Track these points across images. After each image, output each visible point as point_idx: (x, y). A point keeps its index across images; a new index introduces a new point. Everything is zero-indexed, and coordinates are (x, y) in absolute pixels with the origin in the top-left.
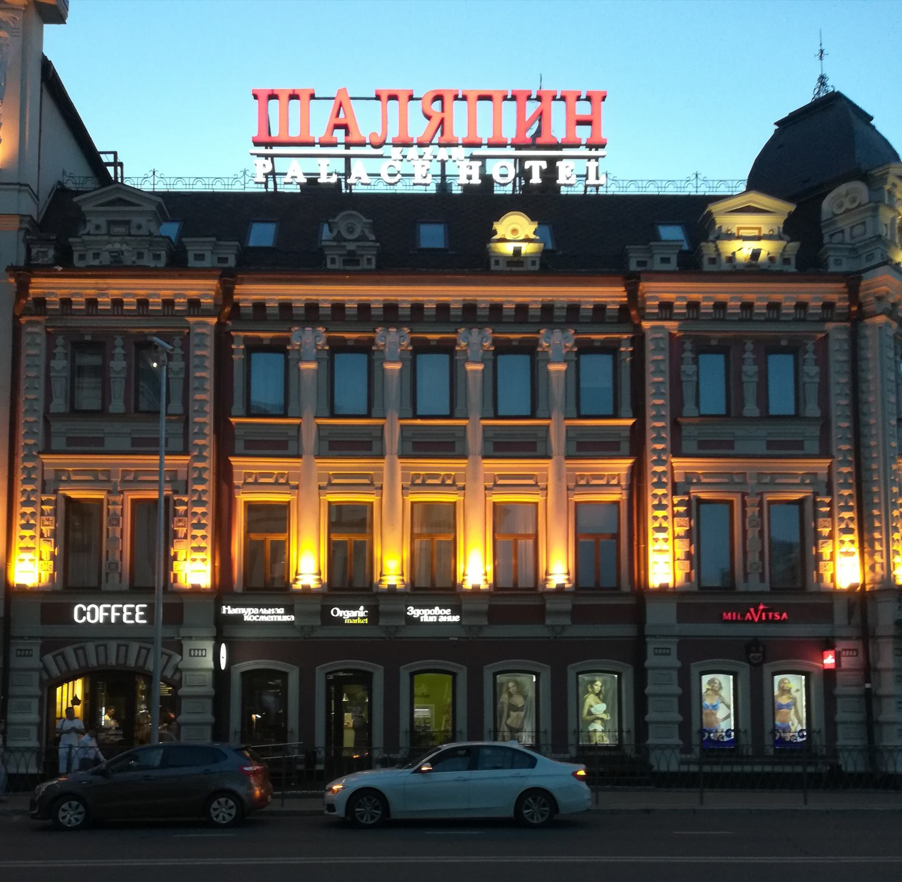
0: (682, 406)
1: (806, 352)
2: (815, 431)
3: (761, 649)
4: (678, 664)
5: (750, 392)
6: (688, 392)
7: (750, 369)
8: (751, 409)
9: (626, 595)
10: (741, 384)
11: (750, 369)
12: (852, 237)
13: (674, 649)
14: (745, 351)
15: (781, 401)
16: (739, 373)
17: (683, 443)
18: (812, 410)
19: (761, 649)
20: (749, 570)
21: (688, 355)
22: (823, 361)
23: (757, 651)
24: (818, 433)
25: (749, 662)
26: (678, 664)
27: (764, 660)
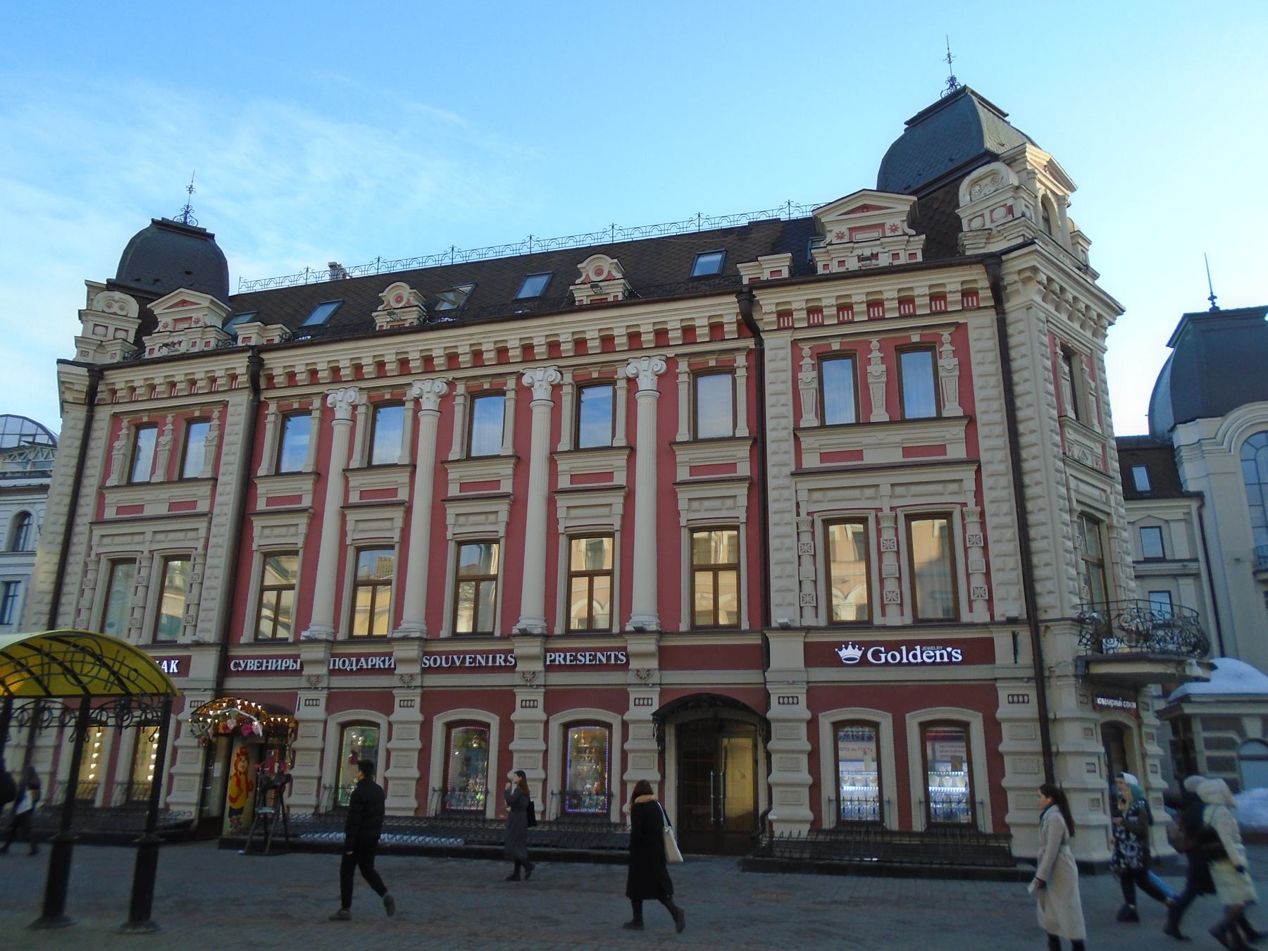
2: (959, 431)
6: (809, 399)
9: (745, 632)
12: (992, 221)
14: (871, 351)
15: (919, 403)
18: (953, 408)
21: (807, 362)
24: (963, 435)
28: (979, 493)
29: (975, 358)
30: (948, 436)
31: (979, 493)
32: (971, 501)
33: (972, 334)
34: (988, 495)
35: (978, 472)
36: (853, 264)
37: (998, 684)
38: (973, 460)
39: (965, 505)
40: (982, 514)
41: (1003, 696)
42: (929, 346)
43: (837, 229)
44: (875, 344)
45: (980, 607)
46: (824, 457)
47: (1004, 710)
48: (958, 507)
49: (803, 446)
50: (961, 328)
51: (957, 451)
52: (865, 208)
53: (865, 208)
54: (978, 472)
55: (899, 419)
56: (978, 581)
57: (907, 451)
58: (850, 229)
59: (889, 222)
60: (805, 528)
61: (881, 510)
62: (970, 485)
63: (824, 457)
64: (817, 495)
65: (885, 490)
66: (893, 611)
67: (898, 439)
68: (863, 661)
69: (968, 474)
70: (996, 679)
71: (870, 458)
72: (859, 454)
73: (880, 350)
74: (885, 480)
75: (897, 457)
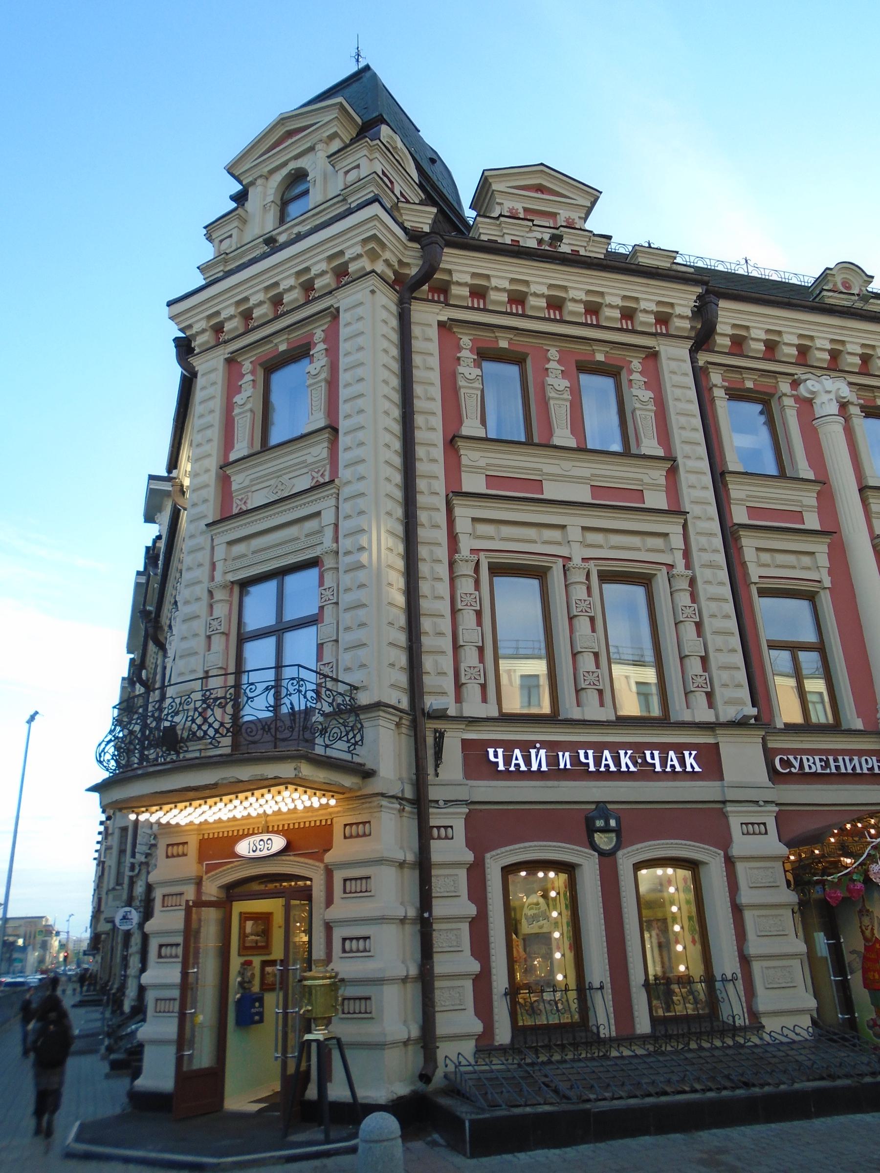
0: (461, 423)
1: (631, 372)
2: (658, 475)
3: (613, 823)
4: (469, 857)
5: (560, 411)
7: (557, 382)
8: (563, 436)
10: (544, 402)
11: (557, 382)
13: (459, 826)
14: (549, 360)
16: (542, 387)
17: (463, 475)
18: (650, 446)
19: (613, 823)
21: (467, 355)
22: (655, 383)
23: (606, 830)
24: (663, 481)
25: (594, 847)
26: (469, 857)
27: (618, 847)
28: (687, 554)
29: (671, 393)
30: (646, 480)
31: (687, 554)
32: (680, 564)
33: (666, 365)
34: (697, 557)
35: (685, 526)
37: (729, 808)
38: (676, 511)
39: (671, 566)
40: (692, 582)
41: (735, 824)
42: (611, 371)
44: (553, 353)
45: (700, 699)
47: (741, 844)
48: (664, 569)
50: (653, 355)
51: (657, 499)
52: (540, 188)
53: (540, 188)
54: (685, 526)
55: (582, 449)
56: (695, 666)
60: (466, 569)
61: (570, 559)
62: (677, 541)
64: (482, 529)
65: (574, 533)
67: (587, 473)
68: (555, 773)
69: (674, 528)
70: (724, 802)
71: (550, 491)
72: (538, 484)
73: (559, 362)
74: (574, 521)
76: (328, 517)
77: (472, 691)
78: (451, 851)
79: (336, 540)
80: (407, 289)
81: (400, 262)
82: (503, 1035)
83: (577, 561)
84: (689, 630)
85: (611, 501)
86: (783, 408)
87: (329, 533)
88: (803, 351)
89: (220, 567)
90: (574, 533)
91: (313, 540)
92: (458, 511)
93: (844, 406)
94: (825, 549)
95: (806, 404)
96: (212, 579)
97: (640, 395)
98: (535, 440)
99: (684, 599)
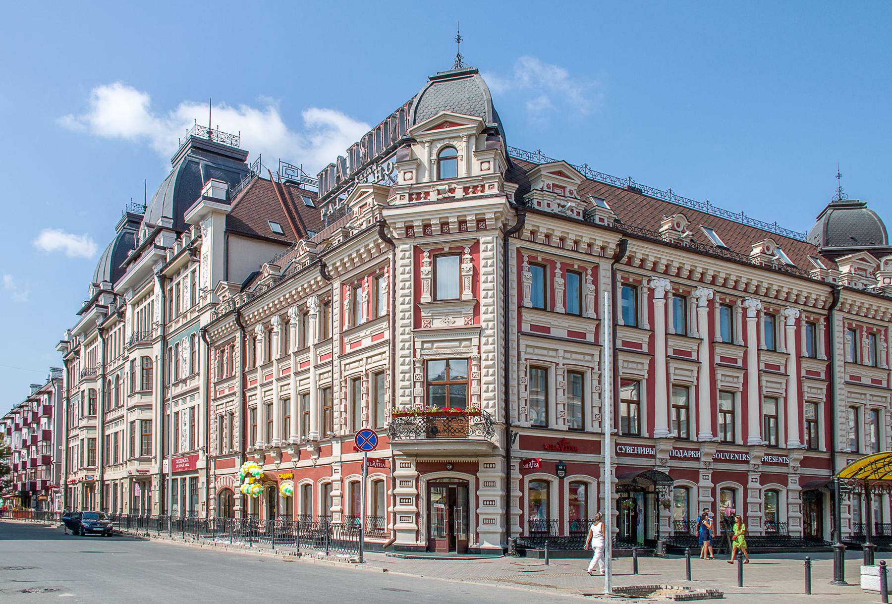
11: (559, 281)
18: (591, 313)
20: (559, 416)
36: (556, 210)
38: (597, 344)
39: (593, 369)
43: (547, 182)
45: (596, 424)
46: (533, 327)
49: (523, 318)
51: (590, 338)
53: (560, 173)
56: (596, 411)
57: (570, 333)
58: (553, 185)
59: (569, 188)
60: (522, 368)
63: (533, 327)
65: (561, 353)
66: (561, 421)
71: (554, 333)
74: (562, 347)
75: (565, 335)
76: (475, 341)
77: (523, 417)
78: (516, 475)
79: (479, 353)
80: (507, 234)
81: (506, 219)
82: (527, 534)
83: (561, 365)
84: (596, 396)
85: (576, 337)
86: (642, 294)
87: (475, 350)
88: (655, 264)
89: (418, 352)
90: (561, 353)
91: (467, 350)
92: (521, 341)
93: (666, 293)
94: (648, 362)
95: (652, 291)
96: (415, 356)
97: (589, 287)
98: (546, 307)
99: (596, 383)
